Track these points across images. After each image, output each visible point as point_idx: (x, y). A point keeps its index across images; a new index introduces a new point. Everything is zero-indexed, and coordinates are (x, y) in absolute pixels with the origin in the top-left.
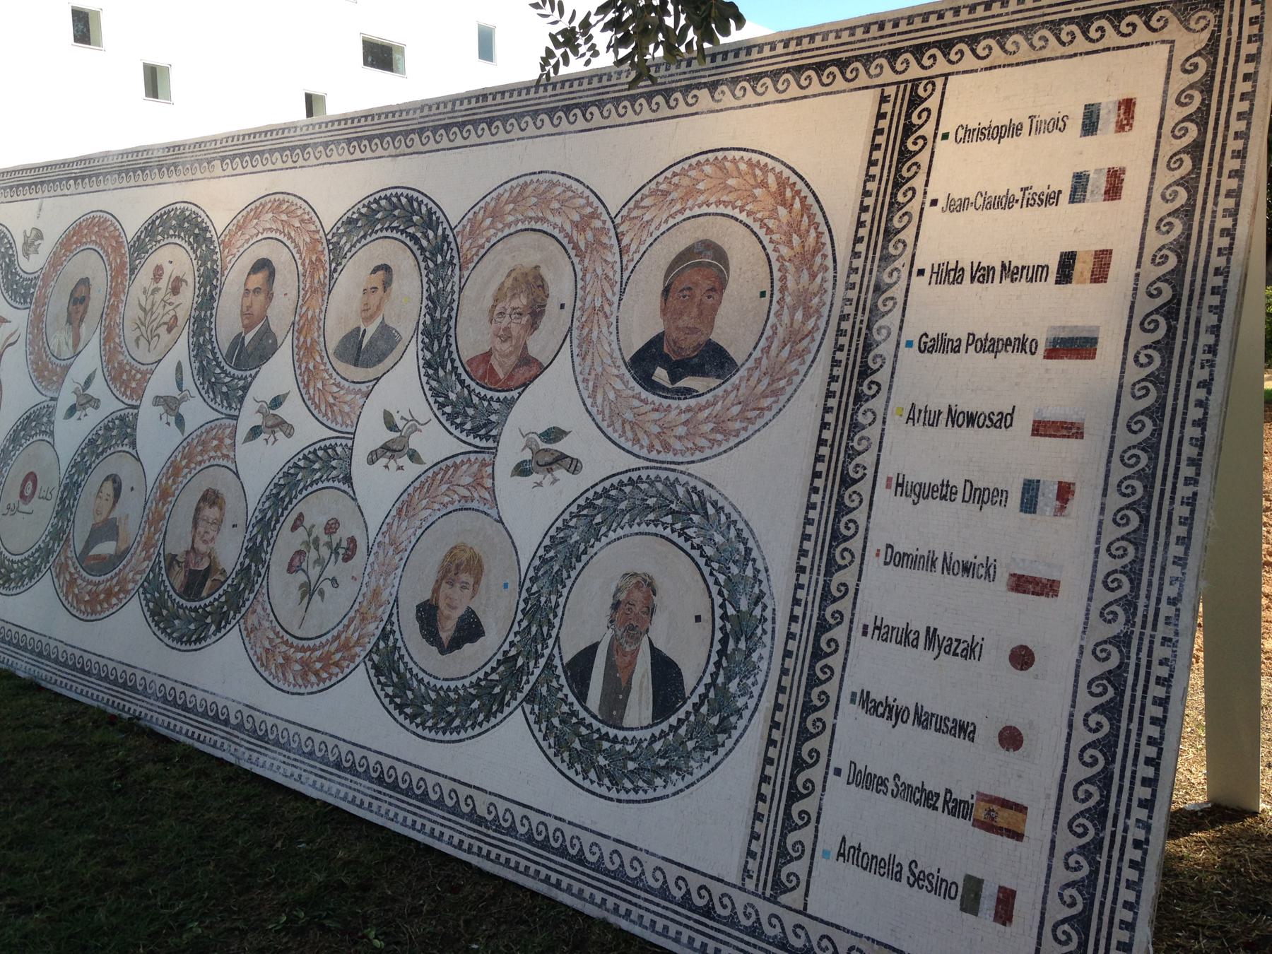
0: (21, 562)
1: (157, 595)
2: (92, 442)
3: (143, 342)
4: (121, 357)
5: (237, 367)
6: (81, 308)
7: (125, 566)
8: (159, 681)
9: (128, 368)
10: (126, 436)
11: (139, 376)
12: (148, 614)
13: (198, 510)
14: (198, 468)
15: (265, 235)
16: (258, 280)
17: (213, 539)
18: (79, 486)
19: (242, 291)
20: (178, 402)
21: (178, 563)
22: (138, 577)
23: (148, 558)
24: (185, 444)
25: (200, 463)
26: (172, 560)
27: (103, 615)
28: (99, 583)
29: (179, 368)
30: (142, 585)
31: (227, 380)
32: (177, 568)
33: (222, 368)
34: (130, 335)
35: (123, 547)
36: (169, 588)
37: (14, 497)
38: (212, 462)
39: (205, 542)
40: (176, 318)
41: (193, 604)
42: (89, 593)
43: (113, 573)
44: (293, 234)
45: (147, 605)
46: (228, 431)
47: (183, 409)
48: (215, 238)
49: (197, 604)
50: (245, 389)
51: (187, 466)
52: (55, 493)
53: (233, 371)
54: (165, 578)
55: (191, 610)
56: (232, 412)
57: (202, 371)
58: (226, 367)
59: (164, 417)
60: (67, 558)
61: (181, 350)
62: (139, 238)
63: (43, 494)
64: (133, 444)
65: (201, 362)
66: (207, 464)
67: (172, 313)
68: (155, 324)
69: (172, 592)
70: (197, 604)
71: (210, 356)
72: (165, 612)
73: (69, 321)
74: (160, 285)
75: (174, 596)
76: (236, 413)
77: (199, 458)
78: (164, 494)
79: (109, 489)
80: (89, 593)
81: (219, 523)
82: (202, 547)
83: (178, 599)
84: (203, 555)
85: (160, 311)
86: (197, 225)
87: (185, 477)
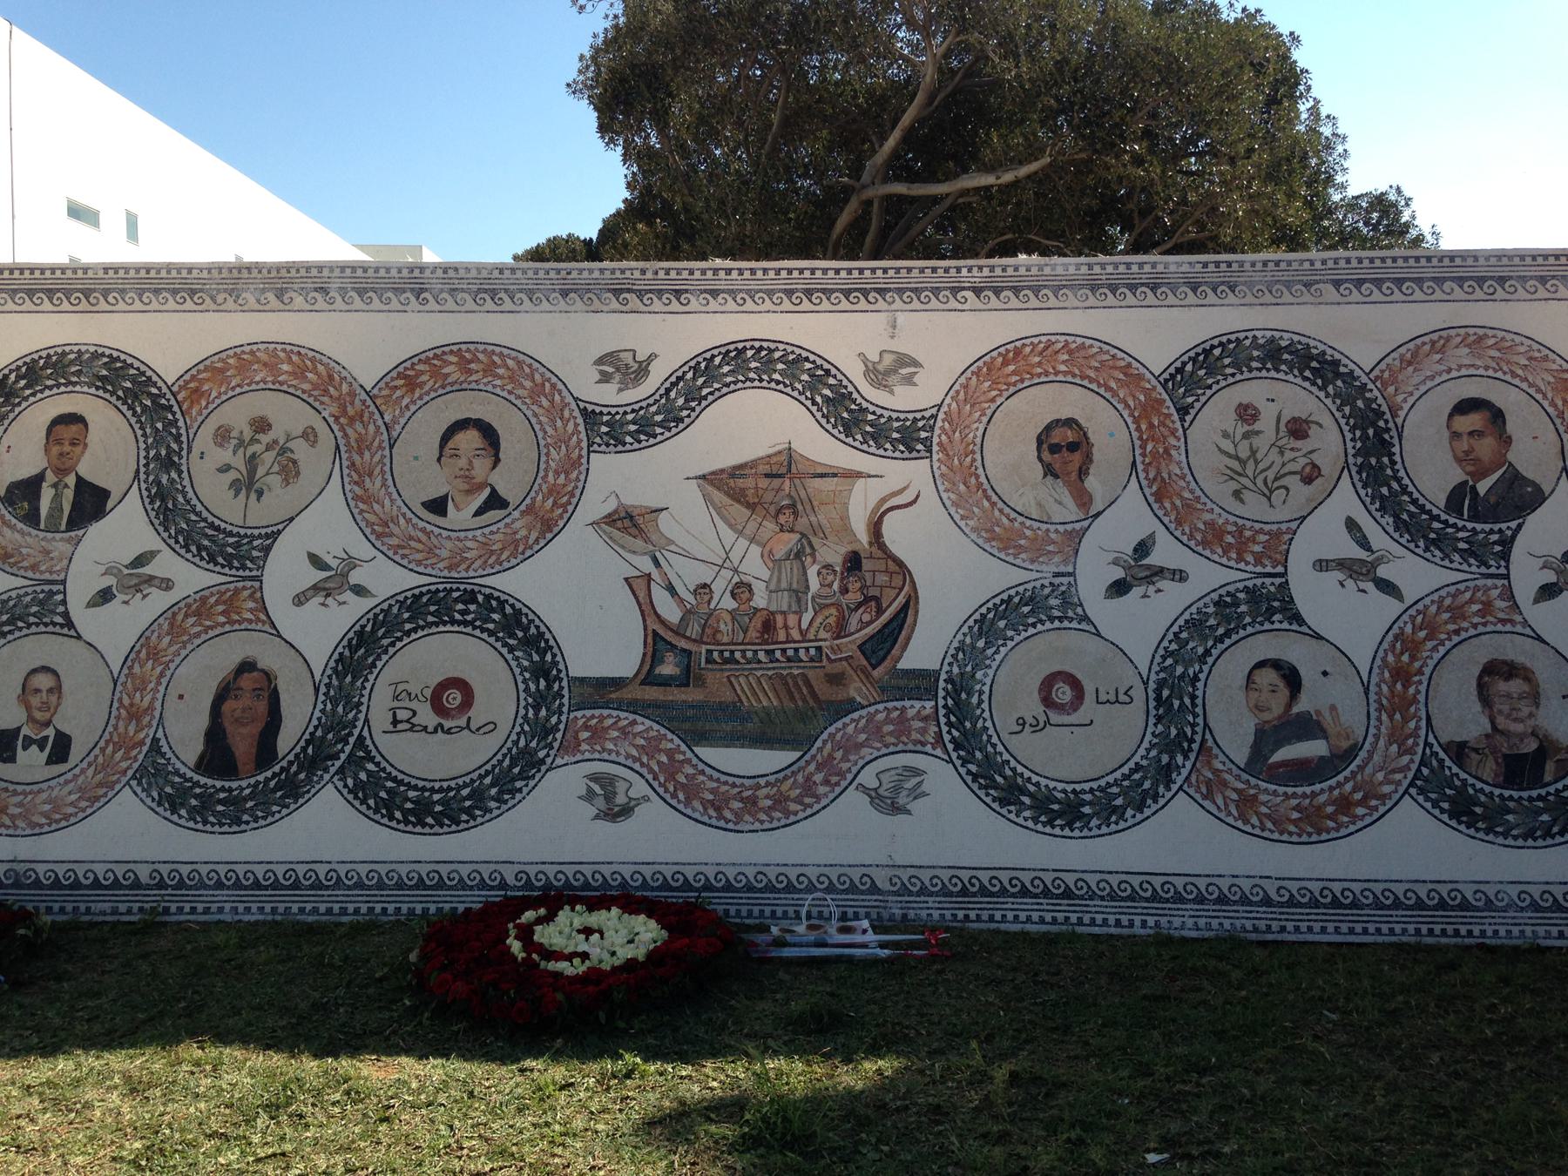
0: (1101, 789)
1: (1448, 791)
2: (1195, 625)
3: (1246, 495)
4: (1207, 517)
5: (1474, 517)
6: (1077, 457)
7: (1361, 768)
8: (1513, 891)
9: (1231, 528)
10: (1271, 612)
11: (1263, 538)
12: (1445, 817)
13: (1481, 686)
14: (1456, 639)
15: (1464, 372)
16: (1474, 421)
17: (1531, 715)
18: (1196, 678)
19: (1446, 434)
20: (1374, 565)
21: (1476, 750)
22: (1398, 776)
23: (1411, 751)
24: (1412, 612)
25: (1457, 632)
26: (1459, 751)
27: (1343, 832)
28: (1314, 795)
29: (1351, 525)
30: (1412, 784)
31: (1461, 535)
32: (1473, 755)
33: (1446, 522)
34: (1218, 490)
35: (1345, 745)
36: (1471, 781)
37: (1032, 707)
38: (1481, 629)
39: (1516, 720)
40: (1314, 466)
41: (1534, 793)
42: (1297, 808)
43: (1340, 777)
44: (1520, 372)
45: (1435, 804)
46: (1494, 593)
47: (1382, 572)
48: (1358, 372)
49: (1543, 792)
50: (1507, 543)
51: (1428, 638)
52: (1138, 693)
53: (1470, 525)
54: (1455, 769)
55: (1531, 799)
56: (1493, 570)
57: (1400, 525)
58: (1452, 521)
59: (1350, 583)
60: (1216, 772)
61: (1346, 500)
62: (1179, 370)
63: (1103, 698)
64: (1297, 618)
65: (1397, 517)
66: (1472, 632)
67: (1303, 461)
68: (1271, 475)
69: (1479, 785)
70: (1543, 792)
71: (1412, 508)
72: (1478, 810)
73: (1049, 471)
74: (1257, 426)
75: (1487, 789)
76: (1503, 571)
77: (1451, 627)
78: (1401, 675)
79: (1268, 677)
80: (1297, 808)
81: (1535, 697)
82: (1518, 728)
83: (1497, 792)
84: (1522, 737)
85: (1274, 455)
86: (1312, 358)
87: (1435, 649)
